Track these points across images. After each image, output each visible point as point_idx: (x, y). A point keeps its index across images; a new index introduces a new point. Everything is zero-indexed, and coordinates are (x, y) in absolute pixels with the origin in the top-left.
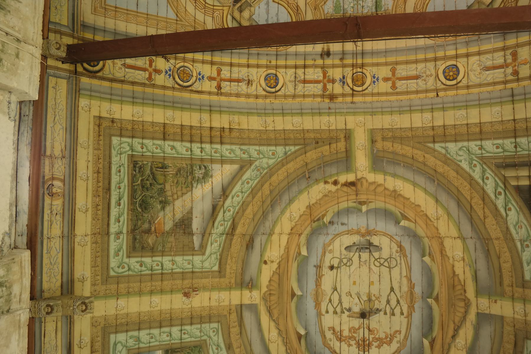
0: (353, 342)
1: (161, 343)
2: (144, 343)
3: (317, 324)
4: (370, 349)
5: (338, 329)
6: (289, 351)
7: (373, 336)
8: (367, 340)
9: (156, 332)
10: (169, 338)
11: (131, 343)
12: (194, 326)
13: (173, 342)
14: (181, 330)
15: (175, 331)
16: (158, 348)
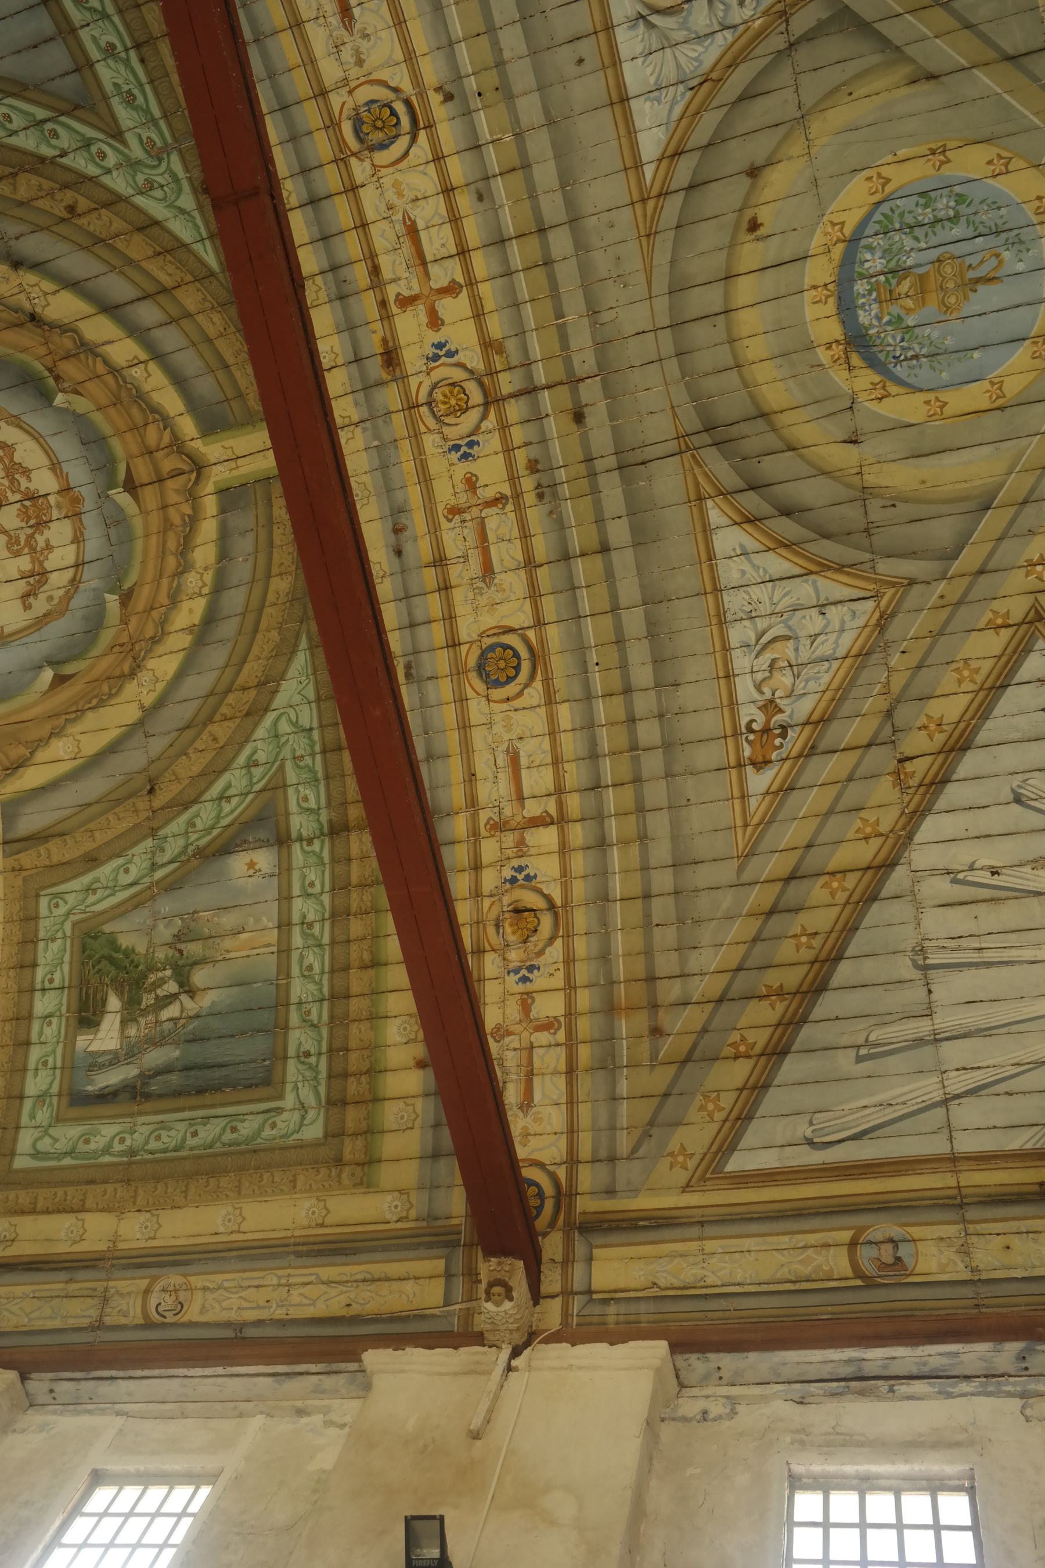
0: (40, 540)
1: (62, 1040)
2: (51, 1084)
3: (24, 640)
4: (41, 493)
5: (22, 586)
6: (95, 702)
7: (9, 494)
8: (23, 505)
9: (35, 1054)
10: (55, 1020)
11: (43, 1116)
12: (41, 960)
13: (64, 1009)
14: (44, 990)
15: (43, 1004)
16: (70, 1043)
